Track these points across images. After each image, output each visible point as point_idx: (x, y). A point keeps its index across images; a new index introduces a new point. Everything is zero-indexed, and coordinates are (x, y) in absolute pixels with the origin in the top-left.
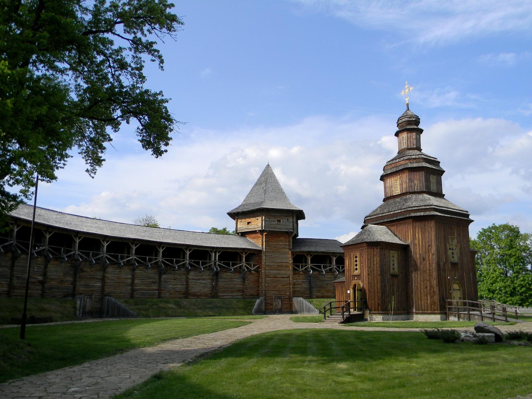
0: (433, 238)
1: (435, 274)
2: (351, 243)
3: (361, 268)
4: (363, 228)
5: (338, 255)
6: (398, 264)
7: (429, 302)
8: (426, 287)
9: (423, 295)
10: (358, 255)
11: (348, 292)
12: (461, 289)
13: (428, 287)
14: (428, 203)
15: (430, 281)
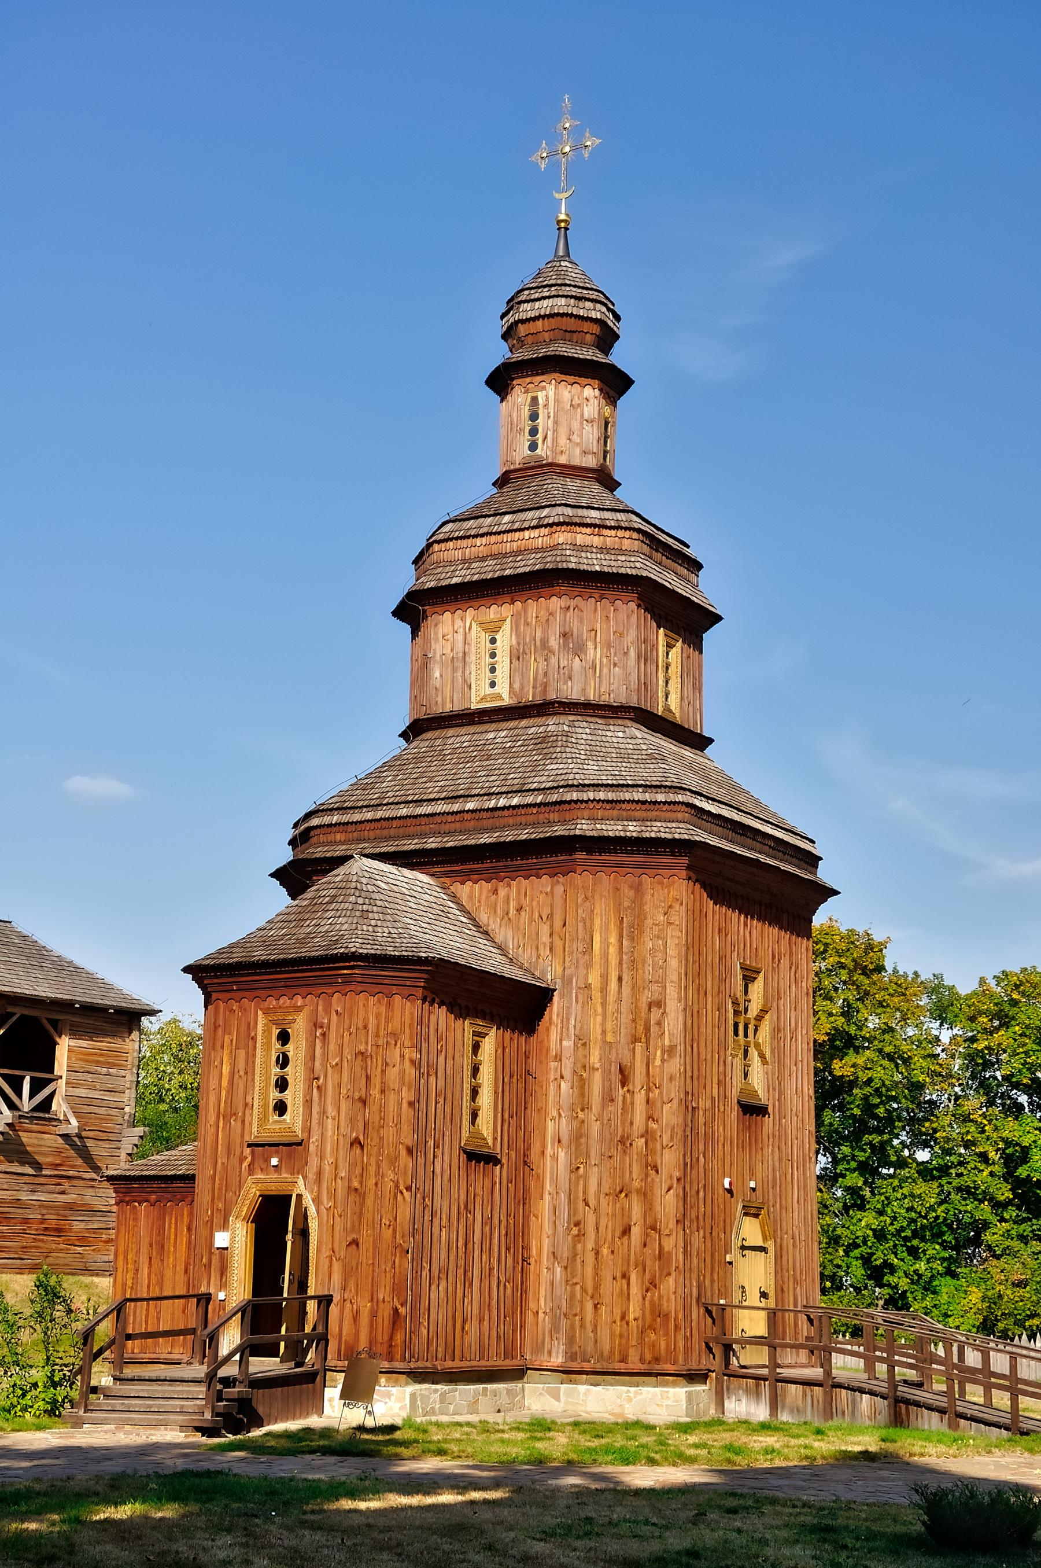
0: (674, 963)
1: (669, 1160)
2: (260, 955)
3: (308, 1103)
4: (294, 878)
5: (18, 1012)
6: (498, 1094)
7: (634, 1310)
8: (626, 1231)
9: (607, 1275)
10: (299, 1028)
11: (221, 1239)
12: (770, 1245)
13: (636, 1231)
14: (652, 773)
15: (645, 1195)
